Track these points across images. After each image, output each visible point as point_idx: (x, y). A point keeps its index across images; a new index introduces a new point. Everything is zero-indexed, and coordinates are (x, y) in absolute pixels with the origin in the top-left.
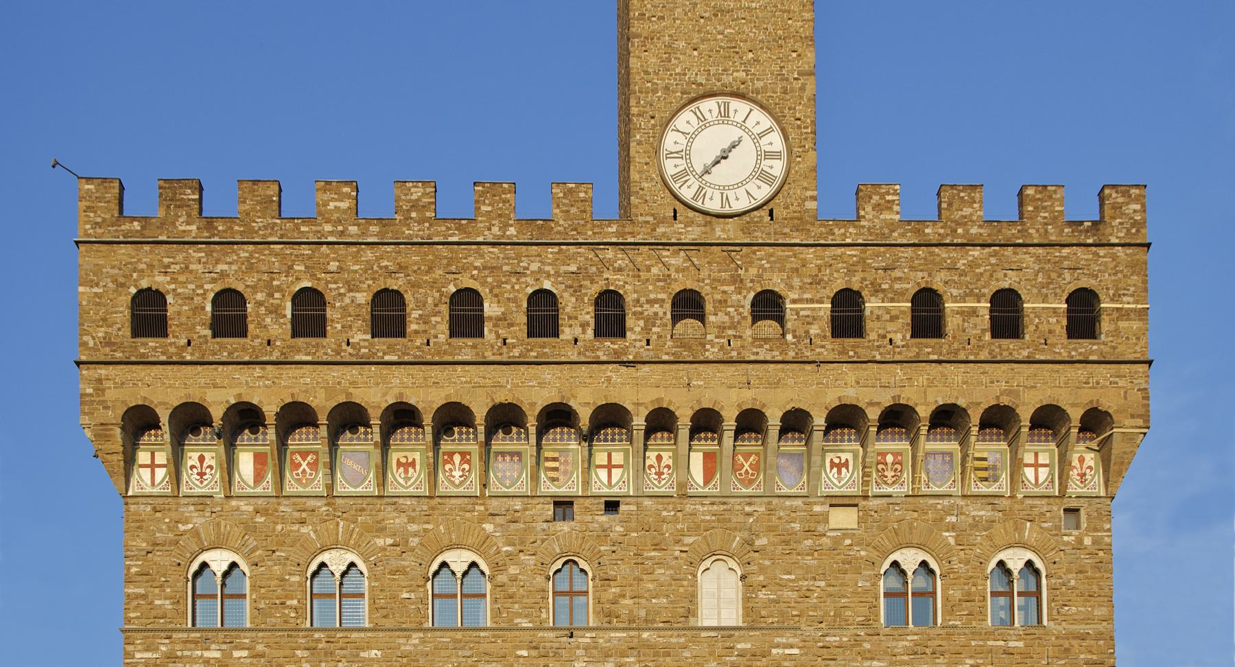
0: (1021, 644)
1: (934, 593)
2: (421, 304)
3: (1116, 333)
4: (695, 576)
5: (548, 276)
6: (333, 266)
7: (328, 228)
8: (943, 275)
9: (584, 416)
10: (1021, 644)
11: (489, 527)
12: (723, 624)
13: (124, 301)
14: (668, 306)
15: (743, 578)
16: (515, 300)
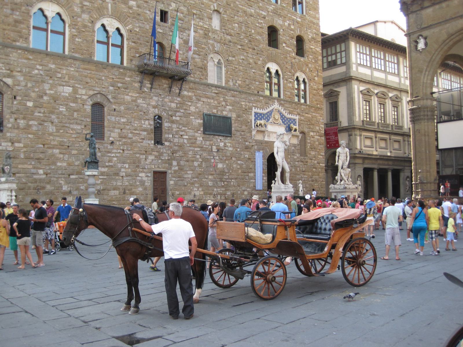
0: (299, 20)
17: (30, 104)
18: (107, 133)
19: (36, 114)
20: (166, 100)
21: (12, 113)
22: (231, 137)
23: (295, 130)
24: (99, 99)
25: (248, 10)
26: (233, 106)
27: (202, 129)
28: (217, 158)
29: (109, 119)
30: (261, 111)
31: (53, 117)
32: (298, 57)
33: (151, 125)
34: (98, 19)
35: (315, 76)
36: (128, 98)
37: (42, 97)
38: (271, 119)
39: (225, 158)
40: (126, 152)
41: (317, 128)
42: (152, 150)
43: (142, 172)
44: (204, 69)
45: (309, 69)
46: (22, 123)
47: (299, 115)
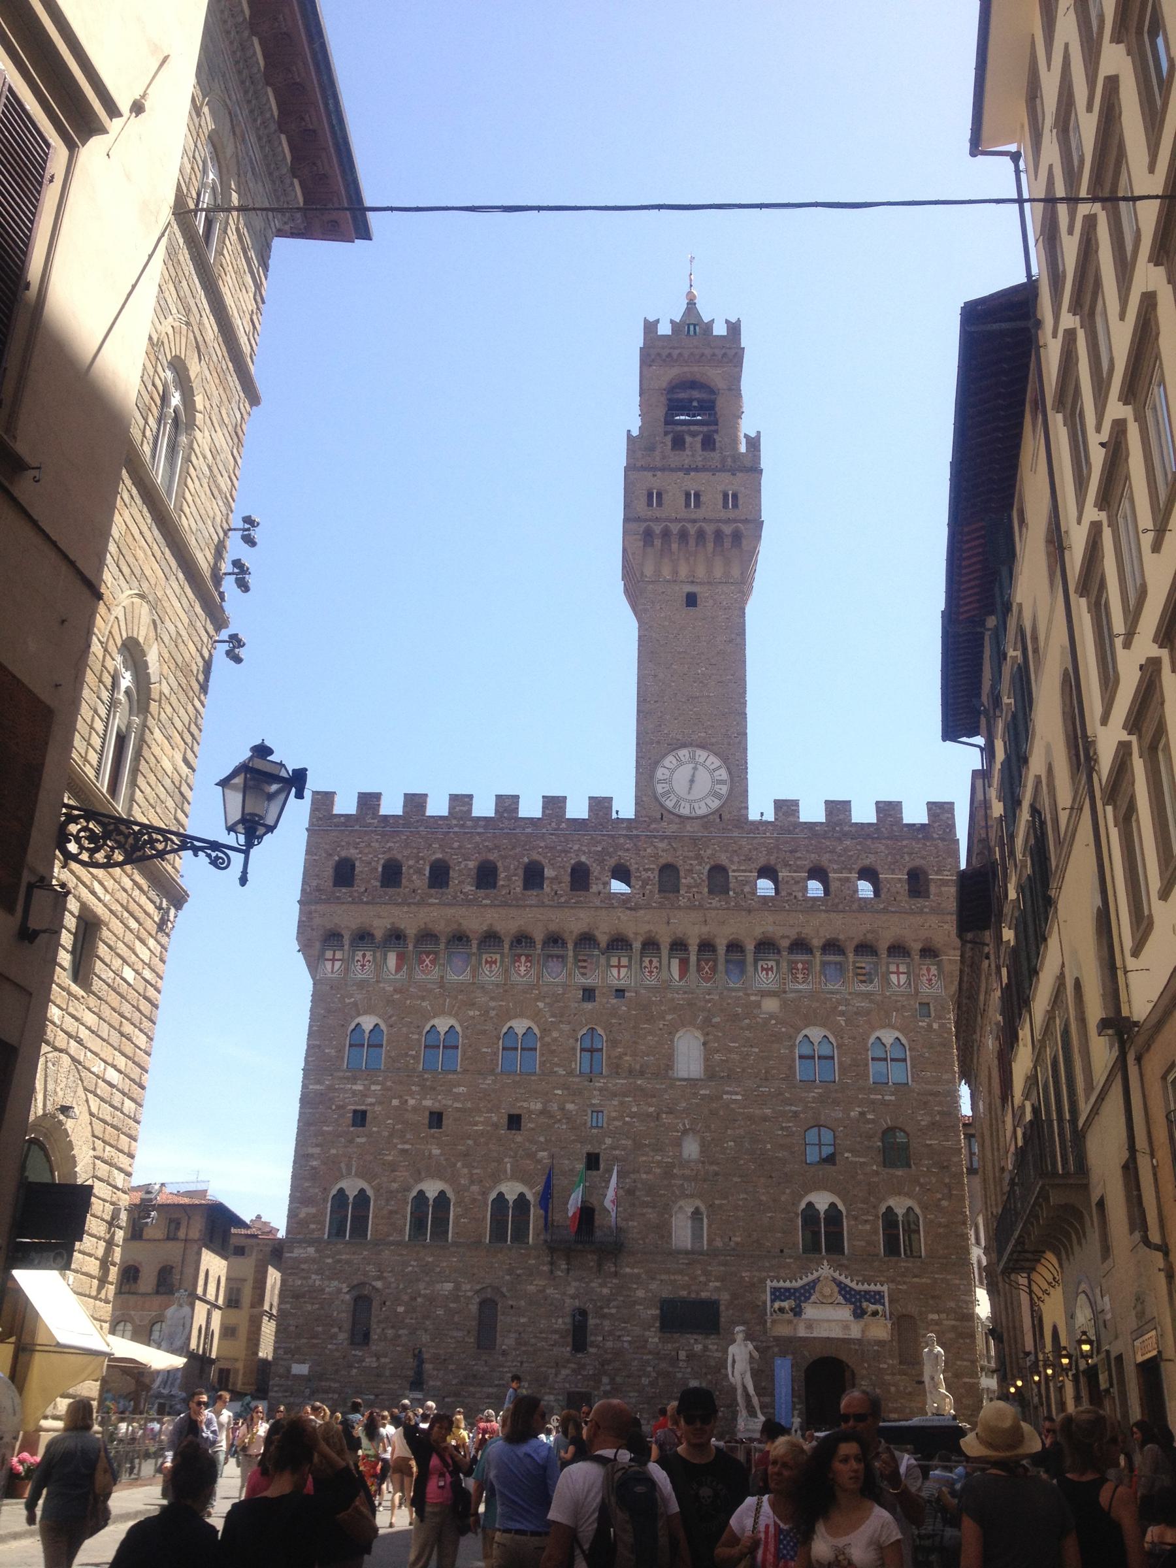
1: (832, 1058)
2: (507, 869)
3: (940, 894)
4: (672, 1041)
5: (584, 853)
6: (456, 845)
7: (455, 822)
8: (827, 856)
9: (603, 940)
10: (893, 1098)
11: (541, 1005)
12: (692, 1076)
13: (331, 864)
14: (657, 872)
15: (704, 1044)
16: (563, 867)
17: (401, 1309)
18: (499, 1340)
19: (407, 1321)
20: (593, 1285)
21: (379, 1322)
22: (718, 1333)
23: (875, 1313)
24: (489, 1294)
25: (757, 1112)
26: (722, 1281)
27: (658, 1325)
28: (689, 1370)
29: (503, 1320)
30: (788, 1284)
31: (427, 1323)
32: (887, 1170)
33: (564, 1323)
34: (491, 1188)
35: (940, 1200)
36: (531, 1288)
37: (415, 1299)
38: (813, 1298)
39: (704, 1370)
40: (525, 1365)
41: (952, 1304)
42: (568, 1361)
43: (550, 1393)
44: (663, 1229)
45: (921, 1186)
46: (390, 1332)
47: (892, 1281)
